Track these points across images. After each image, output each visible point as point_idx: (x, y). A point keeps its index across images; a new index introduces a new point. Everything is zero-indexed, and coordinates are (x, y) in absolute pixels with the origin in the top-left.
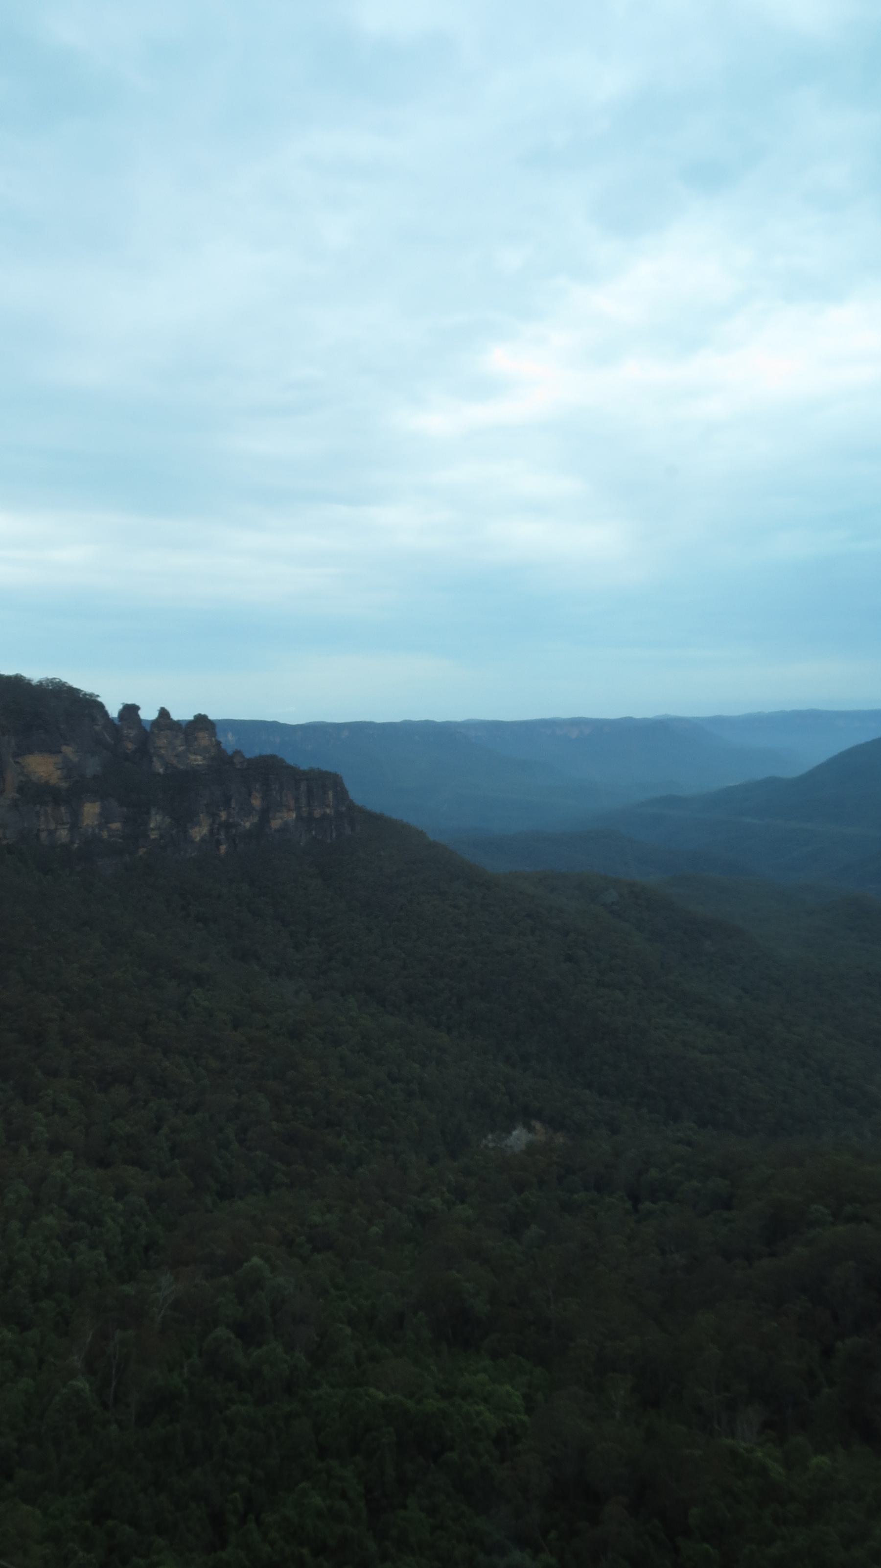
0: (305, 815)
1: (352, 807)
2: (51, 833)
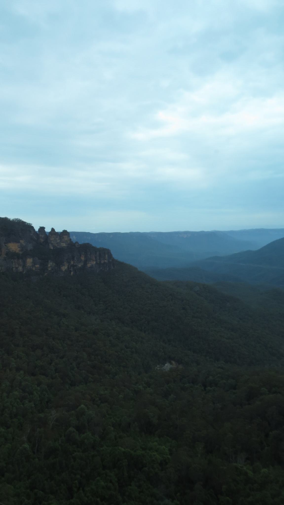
2: (17, 268)
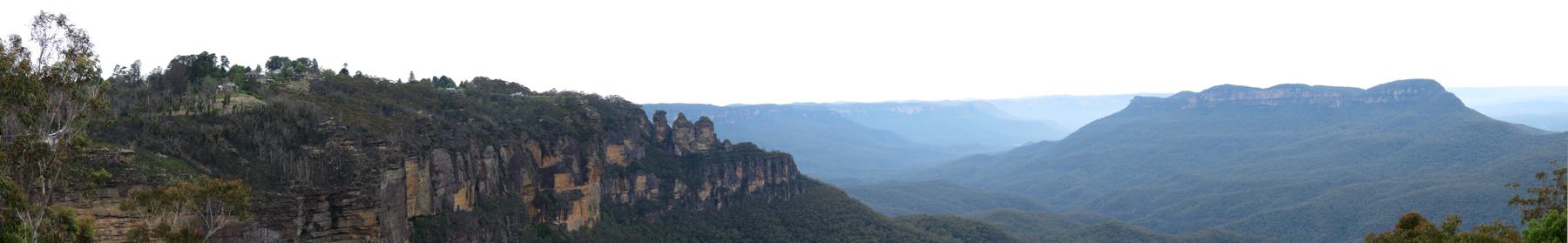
1: (799, 176)
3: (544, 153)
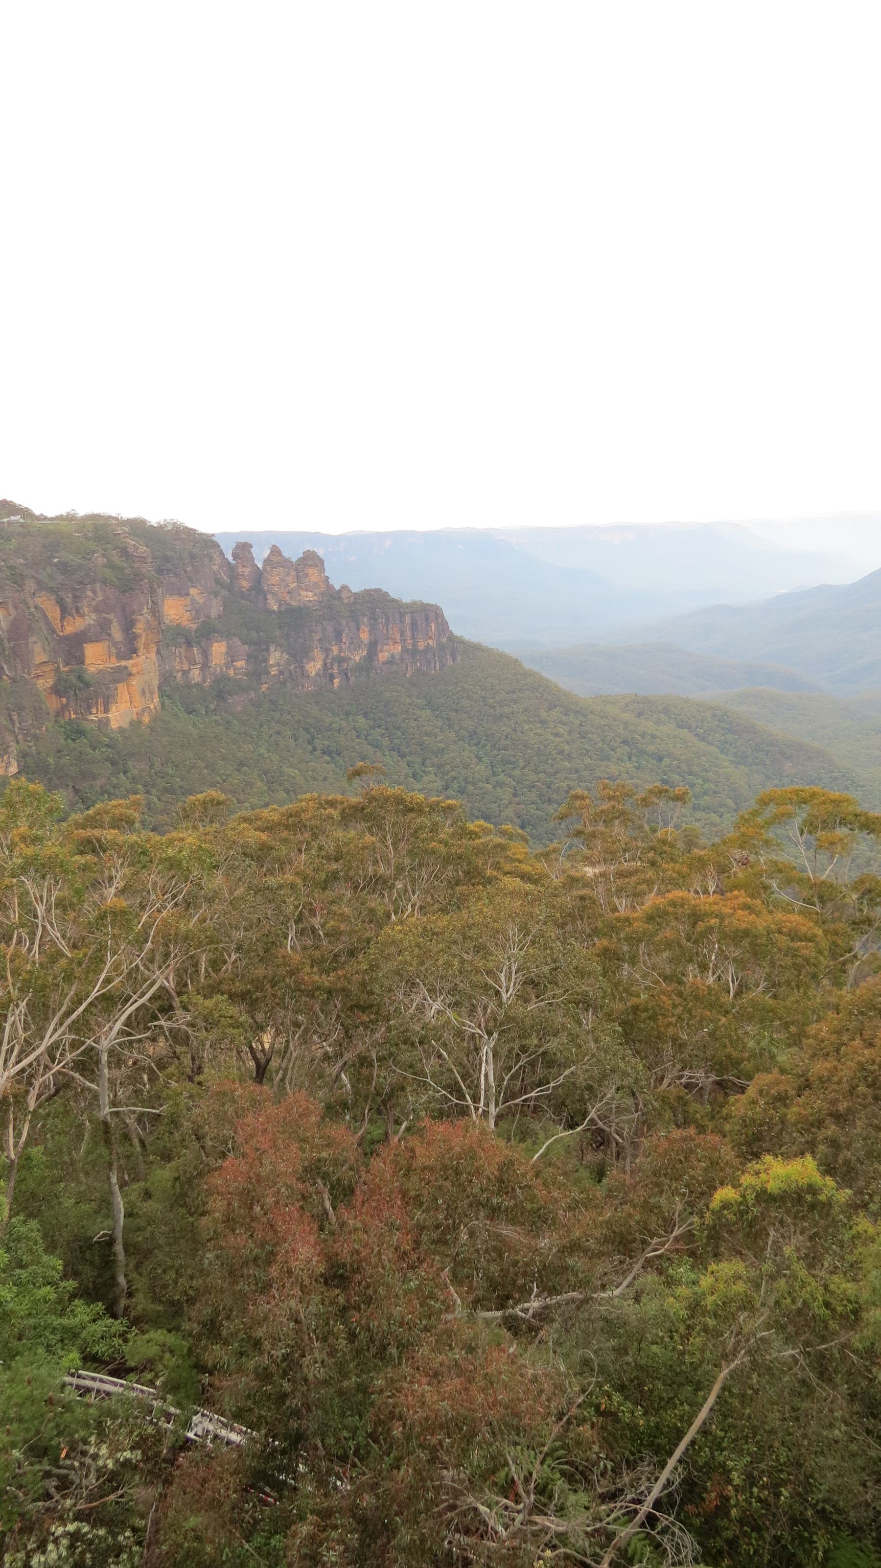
0: (410, 647)
1: (452, 638)
3: (64, 611)
